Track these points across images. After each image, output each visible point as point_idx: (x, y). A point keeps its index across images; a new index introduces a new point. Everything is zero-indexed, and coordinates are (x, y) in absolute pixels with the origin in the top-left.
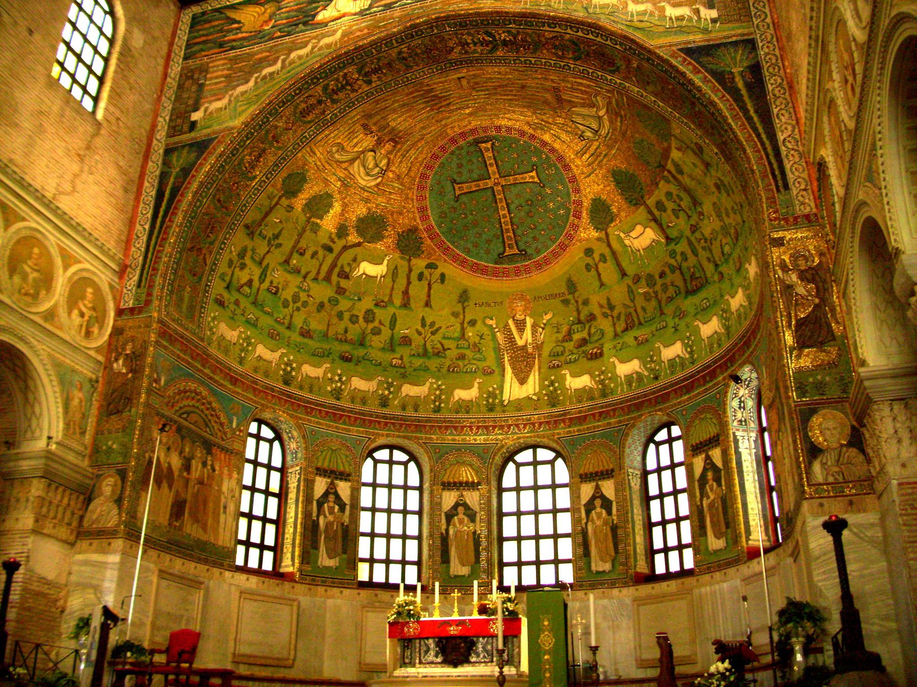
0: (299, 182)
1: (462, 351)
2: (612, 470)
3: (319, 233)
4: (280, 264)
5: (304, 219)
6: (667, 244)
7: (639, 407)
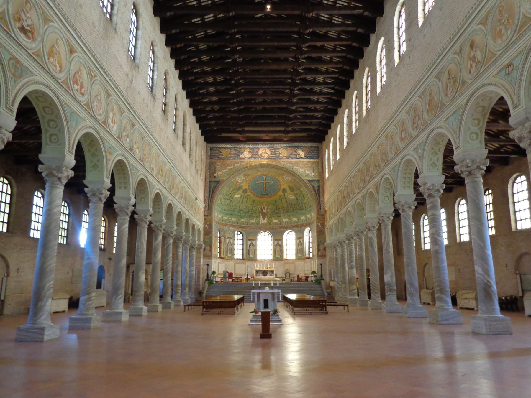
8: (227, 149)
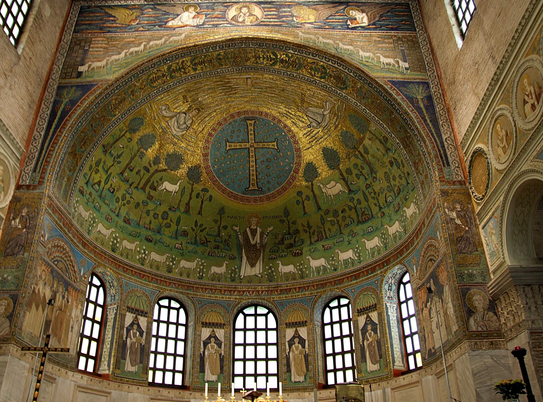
0: (139, 124)
1: (218, 244)
2: (306, 322)
3: (144, 159)
4: (117, 174)
5: (137, 148)
6: (349, 194)
7: (323, 285)
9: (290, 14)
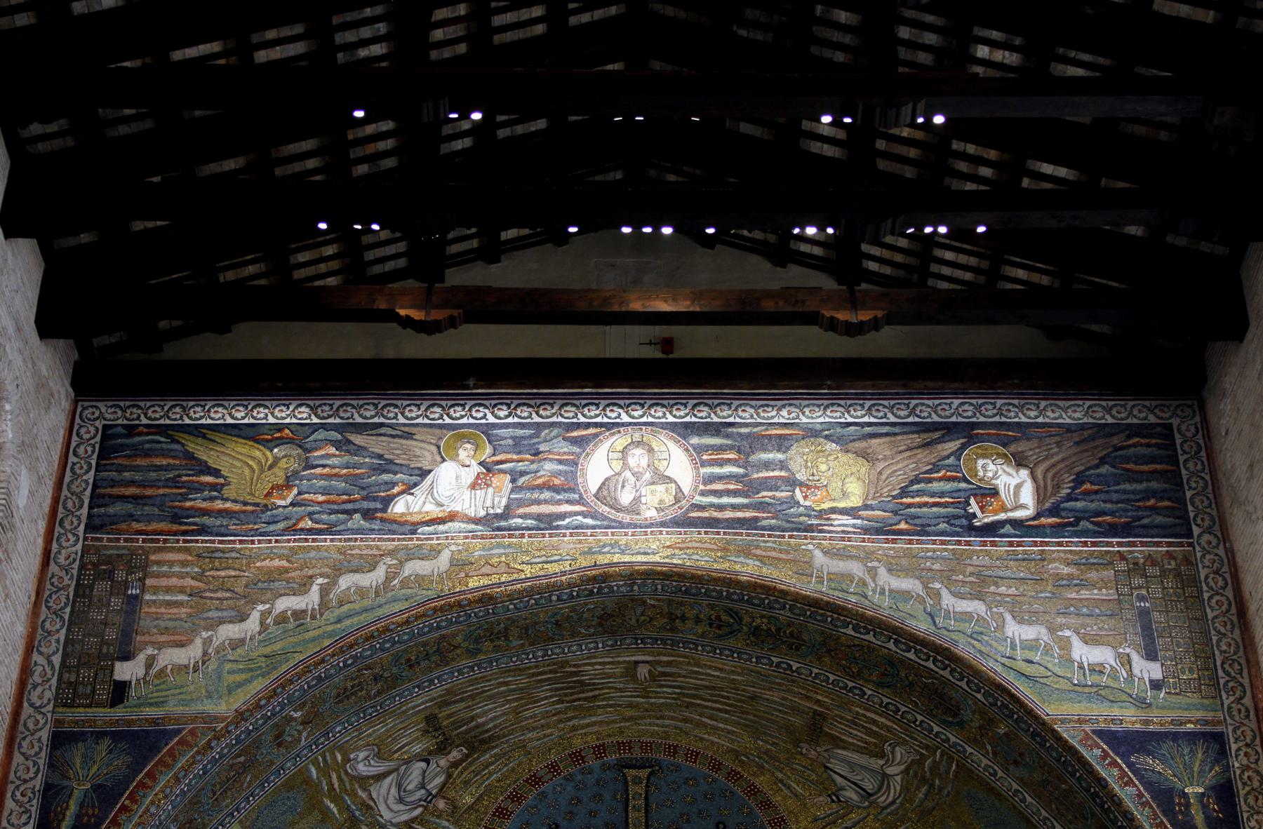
8: (269, 444)
9: (783, 474)
